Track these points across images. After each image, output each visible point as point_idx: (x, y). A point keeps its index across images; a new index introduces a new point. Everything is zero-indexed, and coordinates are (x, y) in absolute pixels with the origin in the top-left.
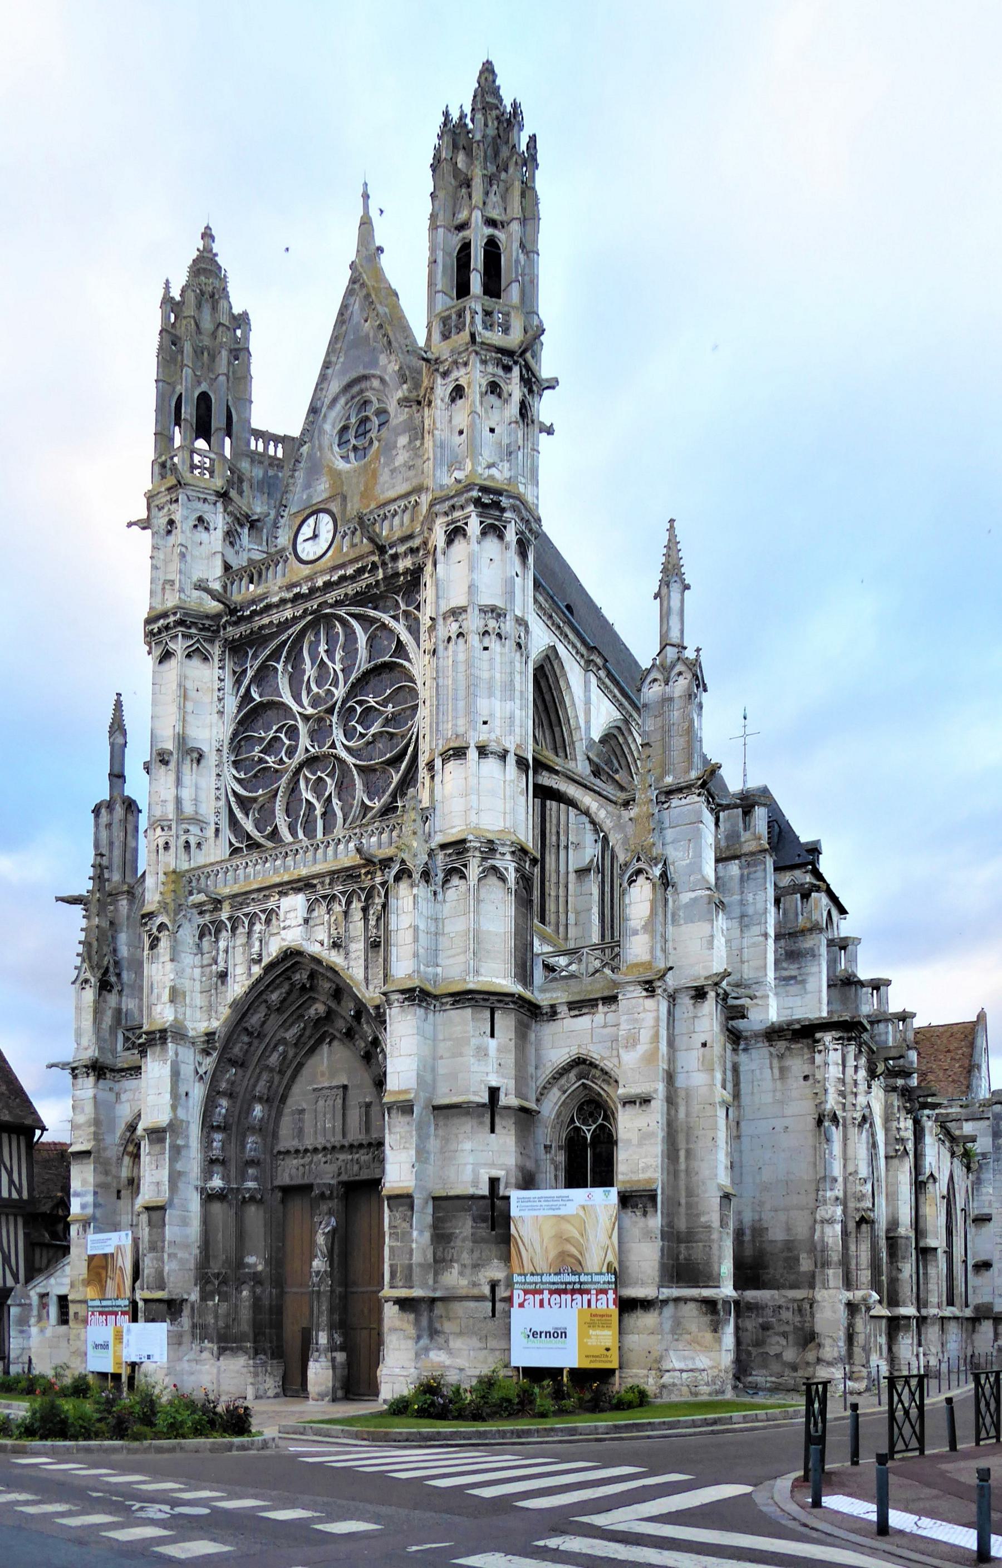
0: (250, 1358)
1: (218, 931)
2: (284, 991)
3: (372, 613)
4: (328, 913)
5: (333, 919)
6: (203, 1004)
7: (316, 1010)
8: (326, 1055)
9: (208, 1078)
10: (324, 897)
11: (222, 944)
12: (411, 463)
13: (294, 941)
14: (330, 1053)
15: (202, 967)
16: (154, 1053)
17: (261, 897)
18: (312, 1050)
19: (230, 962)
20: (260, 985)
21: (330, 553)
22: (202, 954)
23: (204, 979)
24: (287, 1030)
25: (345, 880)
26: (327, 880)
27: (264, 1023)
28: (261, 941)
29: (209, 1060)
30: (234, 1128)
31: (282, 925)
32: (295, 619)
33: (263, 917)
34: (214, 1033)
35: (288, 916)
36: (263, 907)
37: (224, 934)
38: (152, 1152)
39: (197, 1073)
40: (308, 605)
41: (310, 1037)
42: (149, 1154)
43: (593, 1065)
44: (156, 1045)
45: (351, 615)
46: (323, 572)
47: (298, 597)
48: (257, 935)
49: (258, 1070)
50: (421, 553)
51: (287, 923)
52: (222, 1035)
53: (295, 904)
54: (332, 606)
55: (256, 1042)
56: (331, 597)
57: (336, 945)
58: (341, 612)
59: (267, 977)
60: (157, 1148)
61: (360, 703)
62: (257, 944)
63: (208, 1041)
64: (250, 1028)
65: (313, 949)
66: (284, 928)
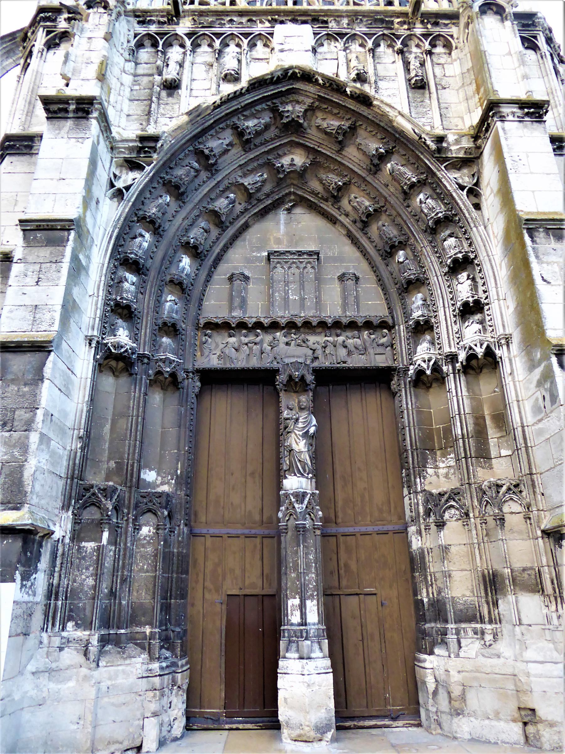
0: (152, 659)
1: (168, 45)
2: (263, 121)
4: (345, 50)
6: (131, 113)
7: (292, 160)
8: (282, 222)
9: (131, 196)
15: (135, 75)
16: (60, 129)
18: (264, 213)
20: (235, 103)
22: (137, 64)
23: (137, 87)
24: (245, 175)
25: (371, 24)
27: (226, 151)
29: (132, 175)
30: (152, 273)
39: (112, 185)
41: (268, 196)
49: (196, 212)
51: (285, 47)
52: (166, 147)
55: (204, 175)
59: (252, 95)
60: (45, 253)
63: (140, 150)
64: (207, 152)
66: (282, 51)
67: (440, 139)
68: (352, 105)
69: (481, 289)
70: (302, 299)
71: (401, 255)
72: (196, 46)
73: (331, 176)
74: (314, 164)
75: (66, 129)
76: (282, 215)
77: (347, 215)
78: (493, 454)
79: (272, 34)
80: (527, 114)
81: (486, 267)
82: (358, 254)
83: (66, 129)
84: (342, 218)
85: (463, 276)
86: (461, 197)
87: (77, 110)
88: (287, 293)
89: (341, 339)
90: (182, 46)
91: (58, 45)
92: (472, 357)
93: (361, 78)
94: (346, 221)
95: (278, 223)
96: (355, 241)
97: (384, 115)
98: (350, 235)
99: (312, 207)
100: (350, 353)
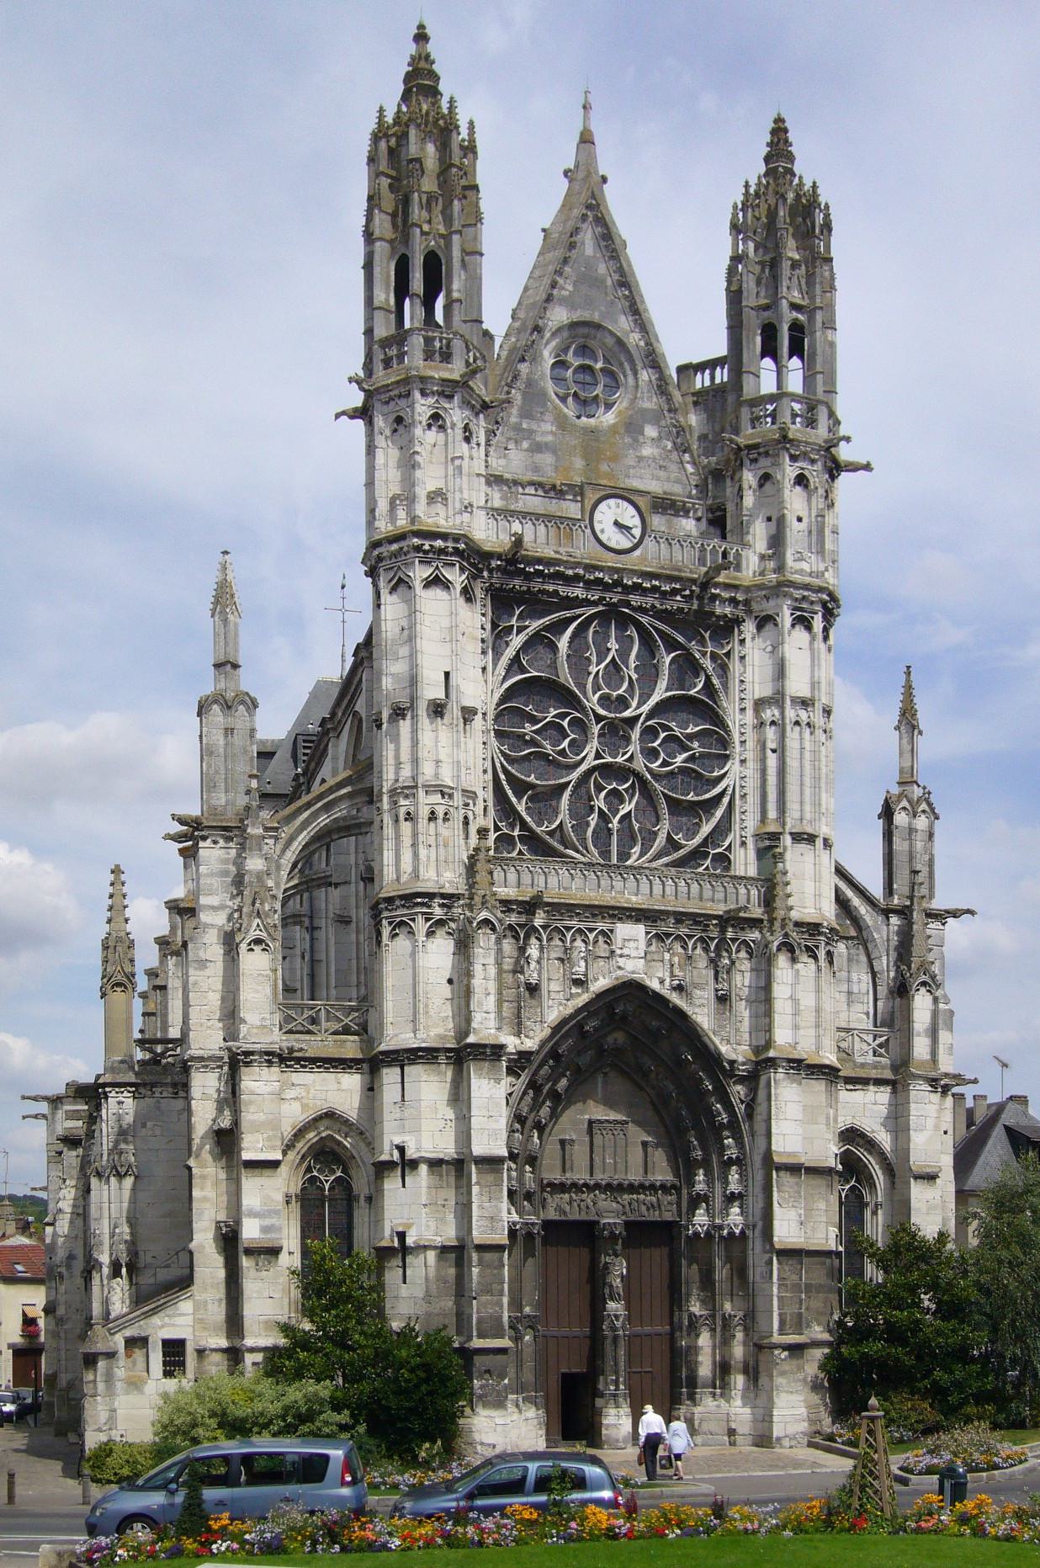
3: (681, 639)
5: (676, 959)
10: (668, 935)
11: (533, 951)
12: (661, 463)
13: (633, 972)
14: (605, 1083)
16: (481, 1069)
19: (545, 976)
21: (637, 553)
28: (586, 961)
33: (591, 936)
34: (530, 1053)
35: (626, 944)
37: (533, 941)
38: (483, 1182)
42: (477, 1183)
43: (863, 1135)
45: (654, 627)
46: (634, 572)
48: (582, 955)
51: (626, 951)
53: (632, 935)
54: (634, 609)
57: (679, 988)
58: (644, 620)
60: (490, 1178)
61: (666, 728)
62: (583, 963)
65: (654, 985)
66: (621, 956)
67: (732, 1062)
72: (550, 939)
75: (485, 1070)
79: (611, 931)
80: (792, 1068)
81: (749, 1169)
83: (485, 1070)
86: (740, 1109)
87: (493, 1054)
88: (604, 1159)
90: (539, 940)
91: (433, 932)
92: (731, 1234)
96: (656, 1110)
98: (652, 1102)
99: (623, 1073)
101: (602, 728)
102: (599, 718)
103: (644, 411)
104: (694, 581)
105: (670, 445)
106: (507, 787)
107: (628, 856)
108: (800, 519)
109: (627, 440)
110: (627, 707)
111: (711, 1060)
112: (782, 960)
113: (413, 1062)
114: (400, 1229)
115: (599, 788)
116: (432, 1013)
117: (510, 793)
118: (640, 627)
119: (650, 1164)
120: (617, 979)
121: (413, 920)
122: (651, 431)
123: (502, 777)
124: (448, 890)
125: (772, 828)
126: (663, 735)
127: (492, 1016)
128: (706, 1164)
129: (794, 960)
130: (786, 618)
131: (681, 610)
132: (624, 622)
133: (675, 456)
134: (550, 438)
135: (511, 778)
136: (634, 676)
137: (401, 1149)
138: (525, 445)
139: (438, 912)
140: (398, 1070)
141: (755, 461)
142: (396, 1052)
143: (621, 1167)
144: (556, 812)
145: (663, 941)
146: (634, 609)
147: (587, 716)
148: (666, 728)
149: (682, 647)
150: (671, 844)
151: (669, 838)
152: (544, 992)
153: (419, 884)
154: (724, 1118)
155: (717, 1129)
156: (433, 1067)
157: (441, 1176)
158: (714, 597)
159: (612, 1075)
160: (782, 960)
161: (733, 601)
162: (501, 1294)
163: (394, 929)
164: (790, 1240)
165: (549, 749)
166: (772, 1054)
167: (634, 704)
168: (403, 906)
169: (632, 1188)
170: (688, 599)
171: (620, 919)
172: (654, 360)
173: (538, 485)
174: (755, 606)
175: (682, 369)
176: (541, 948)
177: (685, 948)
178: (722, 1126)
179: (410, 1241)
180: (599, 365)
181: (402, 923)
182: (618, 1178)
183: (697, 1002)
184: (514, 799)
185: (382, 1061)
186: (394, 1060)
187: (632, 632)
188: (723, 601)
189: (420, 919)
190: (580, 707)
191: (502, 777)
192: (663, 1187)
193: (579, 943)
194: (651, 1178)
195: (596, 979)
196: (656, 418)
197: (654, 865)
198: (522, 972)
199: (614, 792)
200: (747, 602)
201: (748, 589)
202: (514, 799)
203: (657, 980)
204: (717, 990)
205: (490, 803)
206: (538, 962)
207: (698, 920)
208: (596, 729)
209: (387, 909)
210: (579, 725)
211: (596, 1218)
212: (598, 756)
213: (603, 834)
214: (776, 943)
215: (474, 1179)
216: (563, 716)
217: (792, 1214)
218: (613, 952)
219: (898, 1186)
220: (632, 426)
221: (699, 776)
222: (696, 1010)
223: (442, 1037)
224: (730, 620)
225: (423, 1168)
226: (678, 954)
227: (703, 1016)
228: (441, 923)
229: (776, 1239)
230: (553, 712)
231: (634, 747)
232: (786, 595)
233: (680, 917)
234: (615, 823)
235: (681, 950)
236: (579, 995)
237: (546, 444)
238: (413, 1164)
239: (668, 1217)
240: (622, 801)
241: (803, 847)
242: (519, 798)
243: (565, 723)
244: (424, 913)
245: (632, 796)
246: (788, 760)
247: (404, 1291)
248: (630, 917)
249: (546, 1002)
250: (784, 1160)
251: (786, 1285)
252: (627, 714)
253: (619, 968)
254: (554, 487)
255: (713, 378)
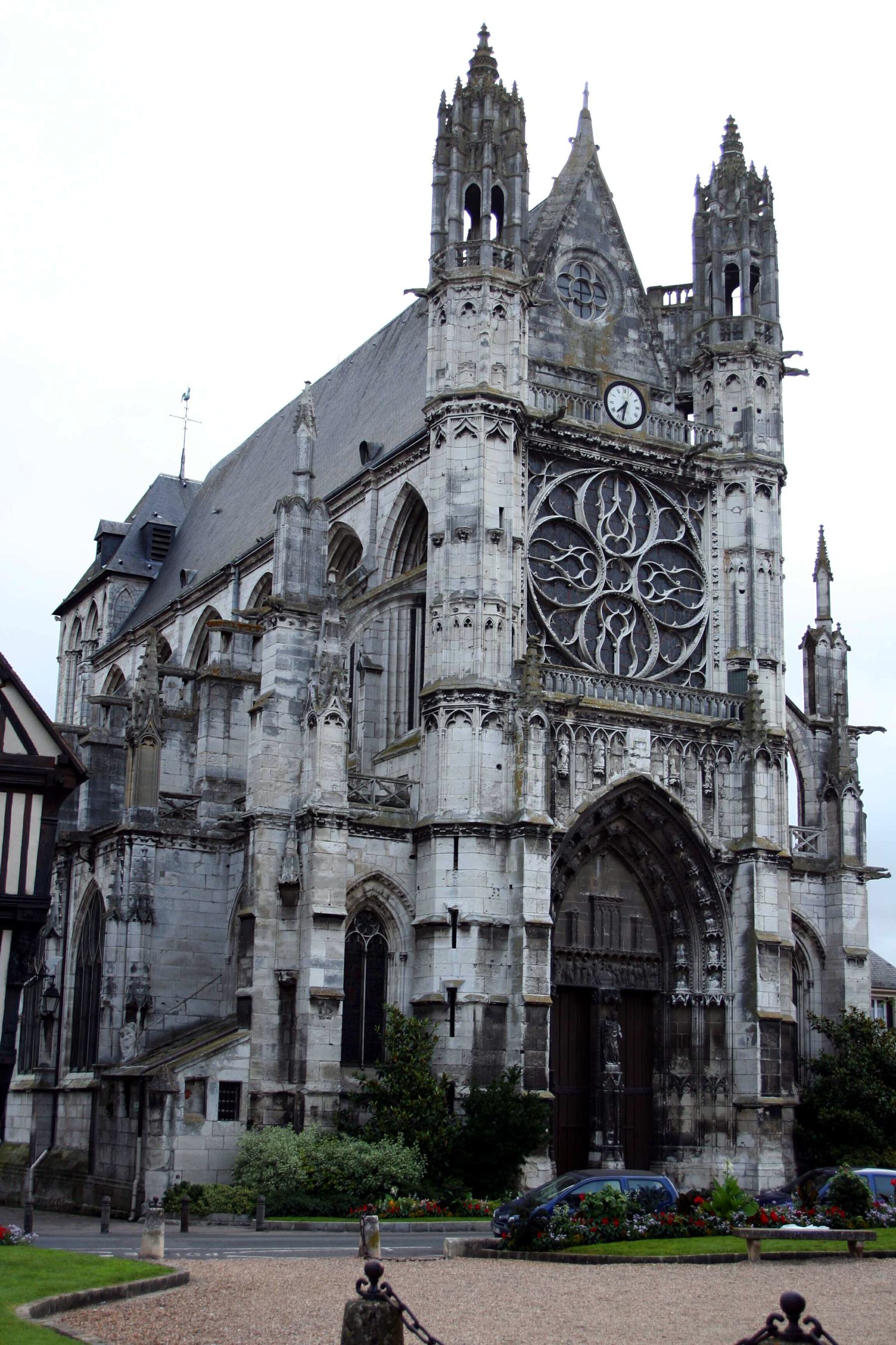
3: (668, 498)
5: (673, 761)
10: (668, 740)
13: (642, 770)
14: (602, 864)
17: (607, 718)
19: (573, 769)
26: (670, 726)
31: (631, 752)
32: (600, 464)
33: (610, 737)
36: (610, 727)
40: (616, 459)
42: (528, 947)
44: (535, 837)
45: (650, 488)
47: (611, 448)
50: (683, 460)
51: (636, 752)
53: (639, 736)
54: (635, 471)
56: (637, 465)
57: (677, 786)
58: (642, 481)
60: (537, 943)
61: (657, 568)
62: (602, 759)
65: (657, 780)
66: (633, 755)
67: (717, 851)
68: (670, 810)
69: (723, 959)
70: (611, 936)
71: (675, 915)
73: (640, 844)
74: (631, 832)
76: (598, 861)
77: (642, 872)
78: (711, 1056)
79: (625, 733)
81: (728, 946)
82: (642, 899)
83: (535, 847)
84: (638, 872)
85: (714, 947)
89: (631, 967)
90: (569, 736)
93: (677, 786)
94: (641, 875)
95: (595, 868)
97: (688, 822)
98: (640, 884)
100: (636, 979)
101: (609, 565)
102: (608, 556)
103: (628, 319)
104: (681, 454)
105: (647, 346)
106: (538, 606)
107: (628, 672)
108: (759, 411)
109: (616, 339)
110: (626, 550)
111: (699, 849)
112: (760, 766)
113: (467, 835)
114: (451, 985)
115: (607, 613)
116: (484, 793)
117: (540, 611)
118: (637, 485)
119: (639, 939)
120: (630, 774)
121: (471, 711)
122: (633, 334)
123: (535, 597)
124: (501, 687)
125: (743, 655)
126: (654, 573)
127: (540, 800)
128: (686, 939)
129: (768, 766)
130: (751, 487)
131: (669, 475)
132: (625, 480)
133: (650, 354)
134: (559, 332)
135: (542, 600)
136: (633, 525)
137: (454, 913)
138: (541, 335)
139: (492, 706)
140: (451, 841)
141: (724, 365)
142: (451, 825)
143: (615, 940)
144: (573, 632)
145: (664, 744)
146: (635, 471)
147: (598, 553)
148: (657, 568)
149: (669, 504)
150: (661, 664)
151: (660, 659)
152: (572, 782)
153: (478, 681)
154: (707, 900)
155: (699, 909)
156: (485, 841)
157: (489, 939)
158: (694, 467)
159: (608, 858)
160: (760, 766)
161: (709, 471)
162: (545, 1050)
163: (451, 717)
164: (769, 1010)
165: (569, 578)
166: (755, 845)
167: (633, 546)
168: (462, 698)
169: (624, 959)
170: (675, 467)
171: (632, 724)
172: (634, 280)
173: (550, 366)
174: (724, 476)
175: (651, 289)
176: (570, 742)
177: (679, 751)
178: (706, 907)
179: (461, 997)
180: (593, 280)
181: (459, 713)
182: (614, 949)
183: (690, 798)
184: (543, 617)
185: (436, 832)
186: (448, 832)
187: (631, 488)
188: (701, 469)
189: (477, 712)
190: (595, 548)
191: (535, 597)
192: (648, 959)
193: (599, 742)
194: (638, 951)
195: (612, 774)
196: (637, 324)
197: (652, 678)
198: (556, 765)
199: (618, 617)
200: (718, 472)
201: (720, 462)
202: (543, 617)
203: (660, 776)
204: (704, 789)
205: (525, 617)
206: (568, 756)
207: (691, 729)
208: (605, 564)
209: (445, 699)
210: (592, 560)
211: (592, 984)
212: (606, 587)
213: (609, 650)
214: (756, 751)
215: (525, 944)
216: (581, 551)
217: (771, 987)
218: (626, 751)
219: (828, 966)
220: (619, 329)
221: (681, 608)
222: (689, 805)
223: (493, 815)
224: (706, 486)
225: (475, 930)
226: (674, 757)
227: (695, 810)
228: (493, 716)
229: (759, 1009)
230: (572, 548)
231: (633, 582)
232: (752, 469)
233: (678, 725)
234: (618, 644)
235: (676, 753)
236: (598, 786)
237: (557, 336)
238: (466, 926)
239: (652, 986)
240: (623, 625)
241: (768, 672)
242: (547, 616)
243: (582, 558)
244: (481, 707)
245: (630, 622)
246: (756, 600)
247: (452, 1043)
248: (640, 722)
249: (574, 791)
250: (765, 939)
251: (767, 1051)
252: (628, 554)
253: (632, 765)
254: (563, 369)
255: (679, 299)
